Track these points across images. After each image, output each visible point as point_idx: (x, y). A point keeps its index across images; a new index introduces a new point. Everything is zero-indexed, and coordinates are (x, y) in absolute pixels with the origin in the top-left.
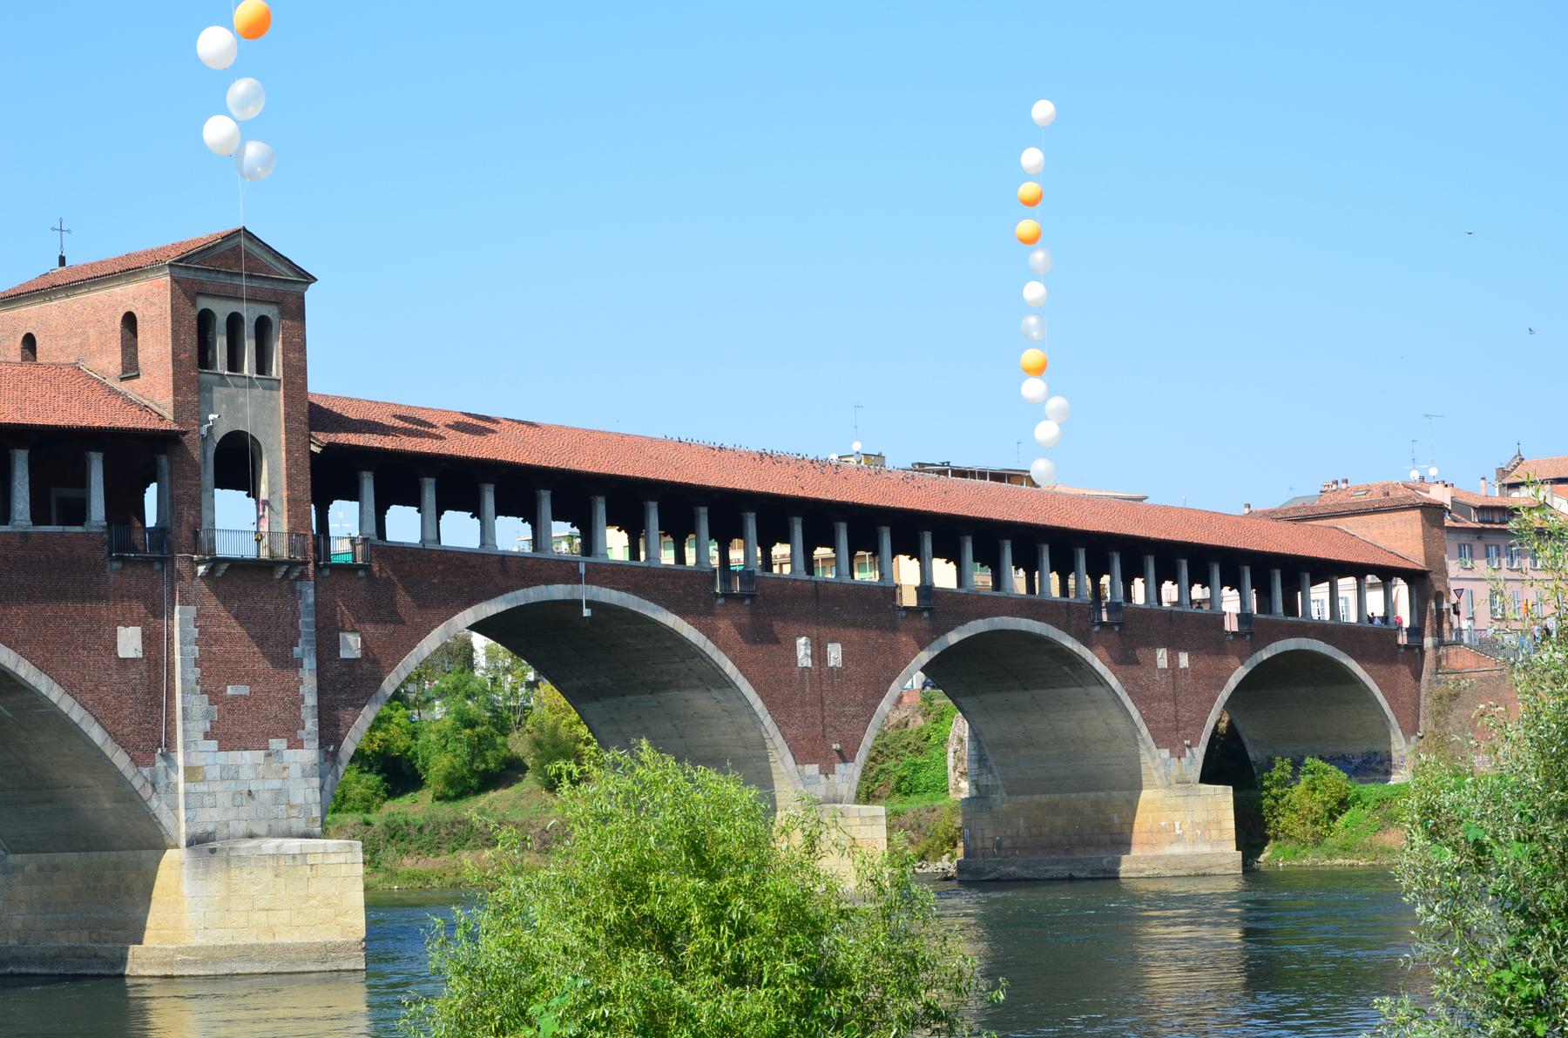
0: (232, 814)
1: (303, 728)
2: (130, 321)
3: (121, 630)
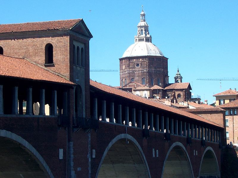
3: (60, 149)
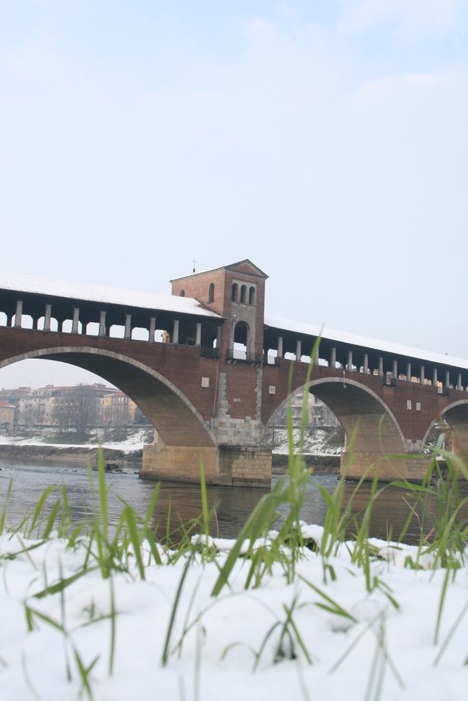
0: (232, 438)
1: (256, 413)
2: (212, 285)
3: (203, 378)
